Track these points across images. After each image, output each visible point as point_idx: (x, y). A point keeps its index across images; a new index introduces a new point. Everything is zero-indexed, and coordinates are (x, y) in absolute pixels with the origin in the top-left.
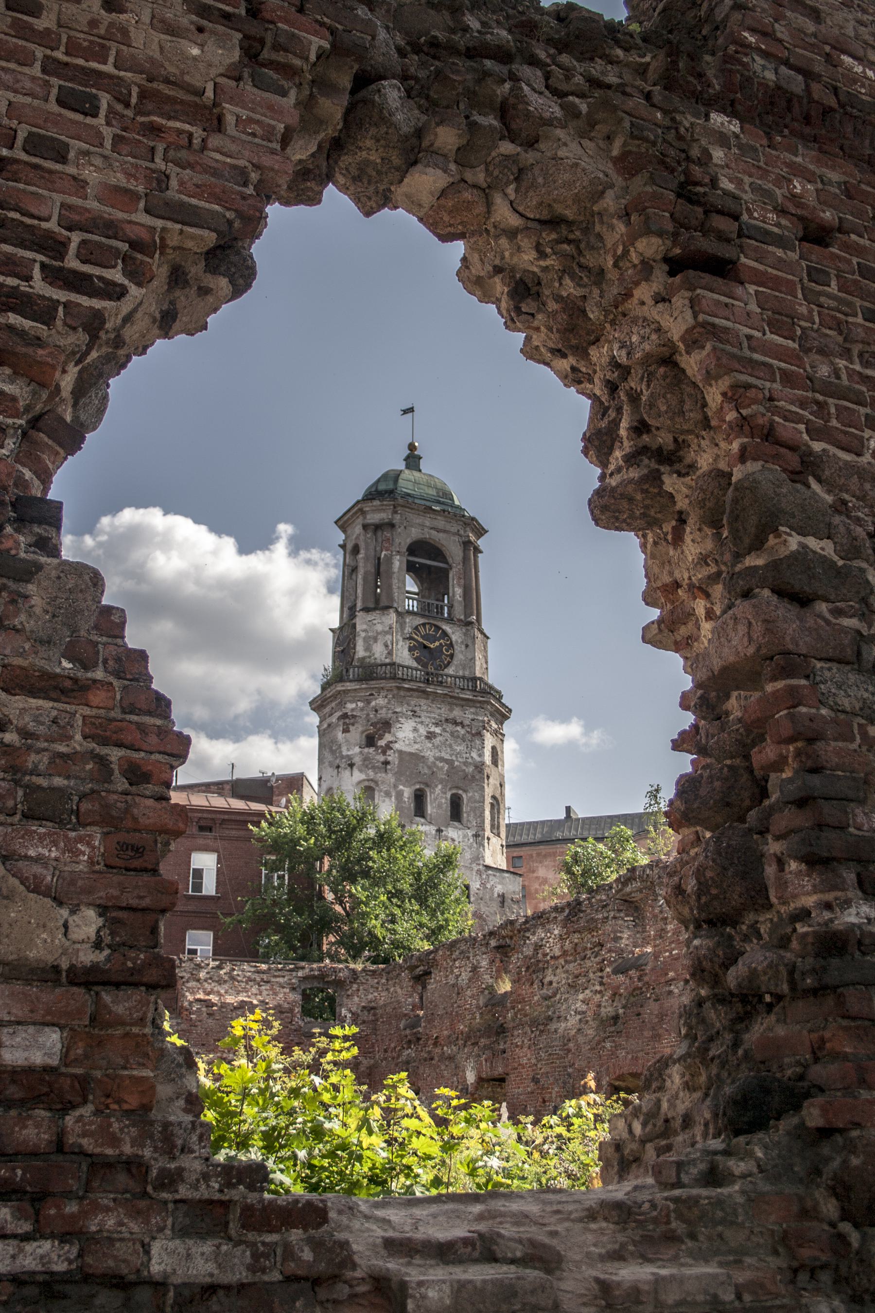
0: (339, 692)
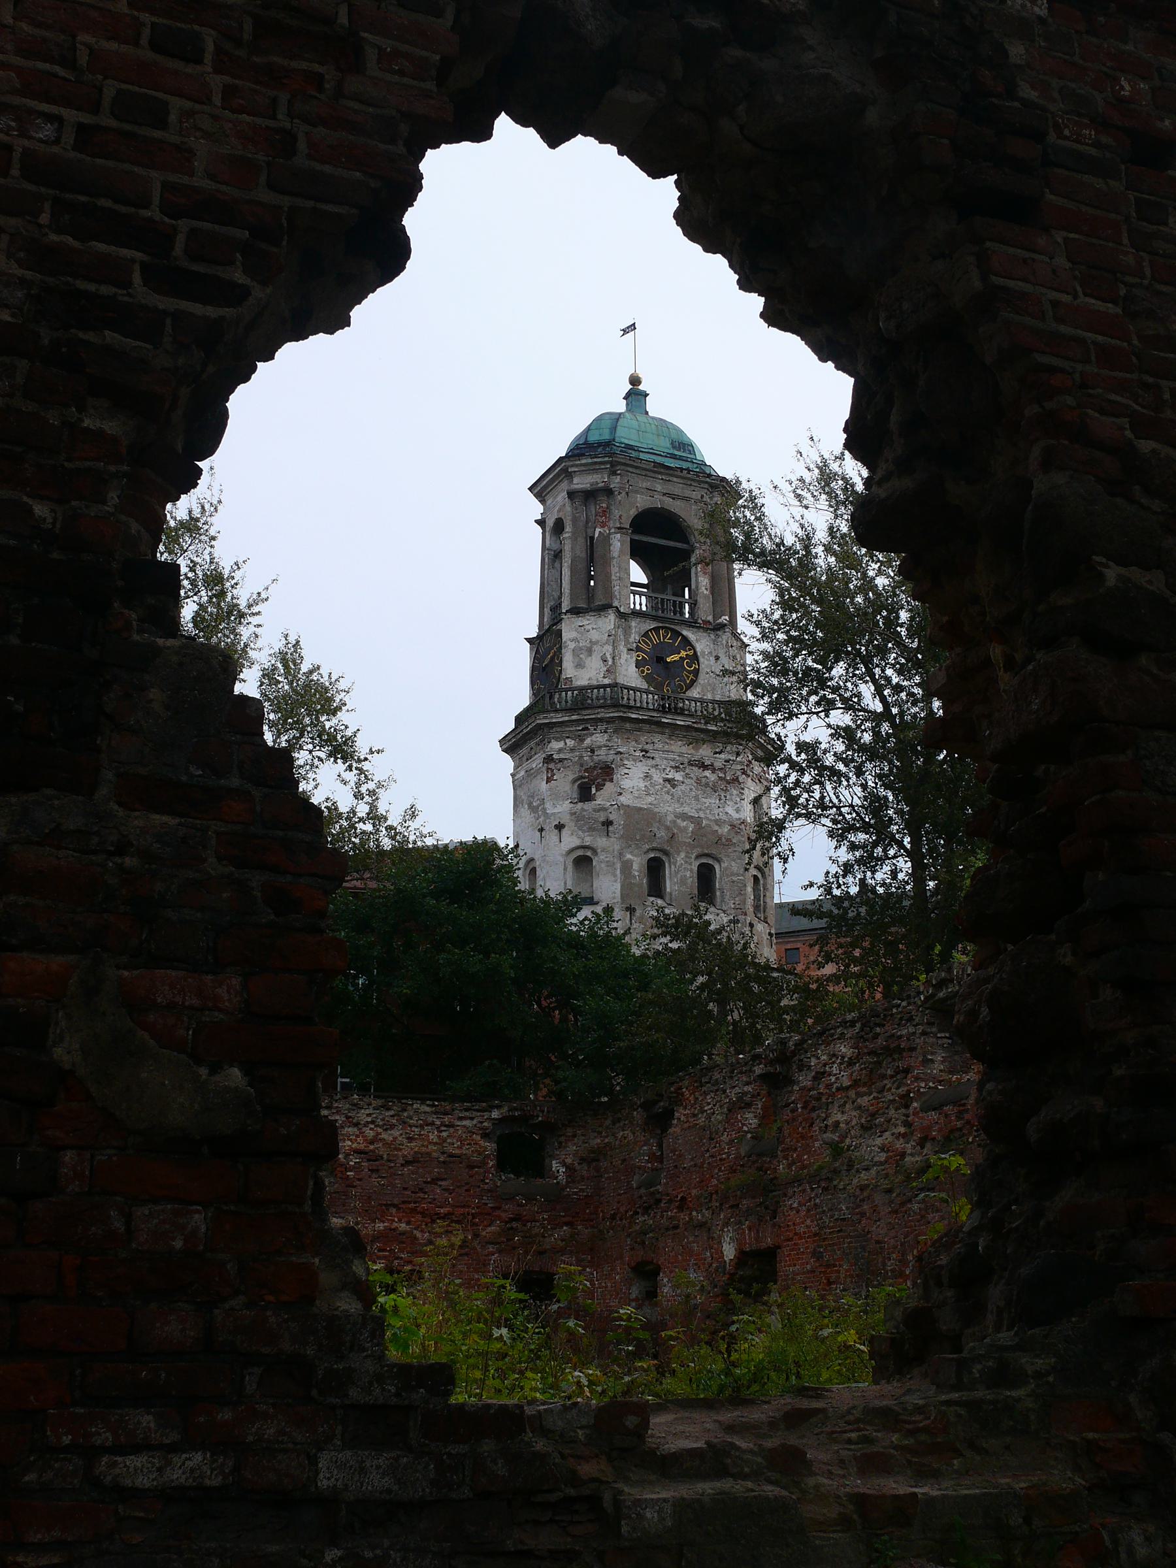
0: (540, 727)
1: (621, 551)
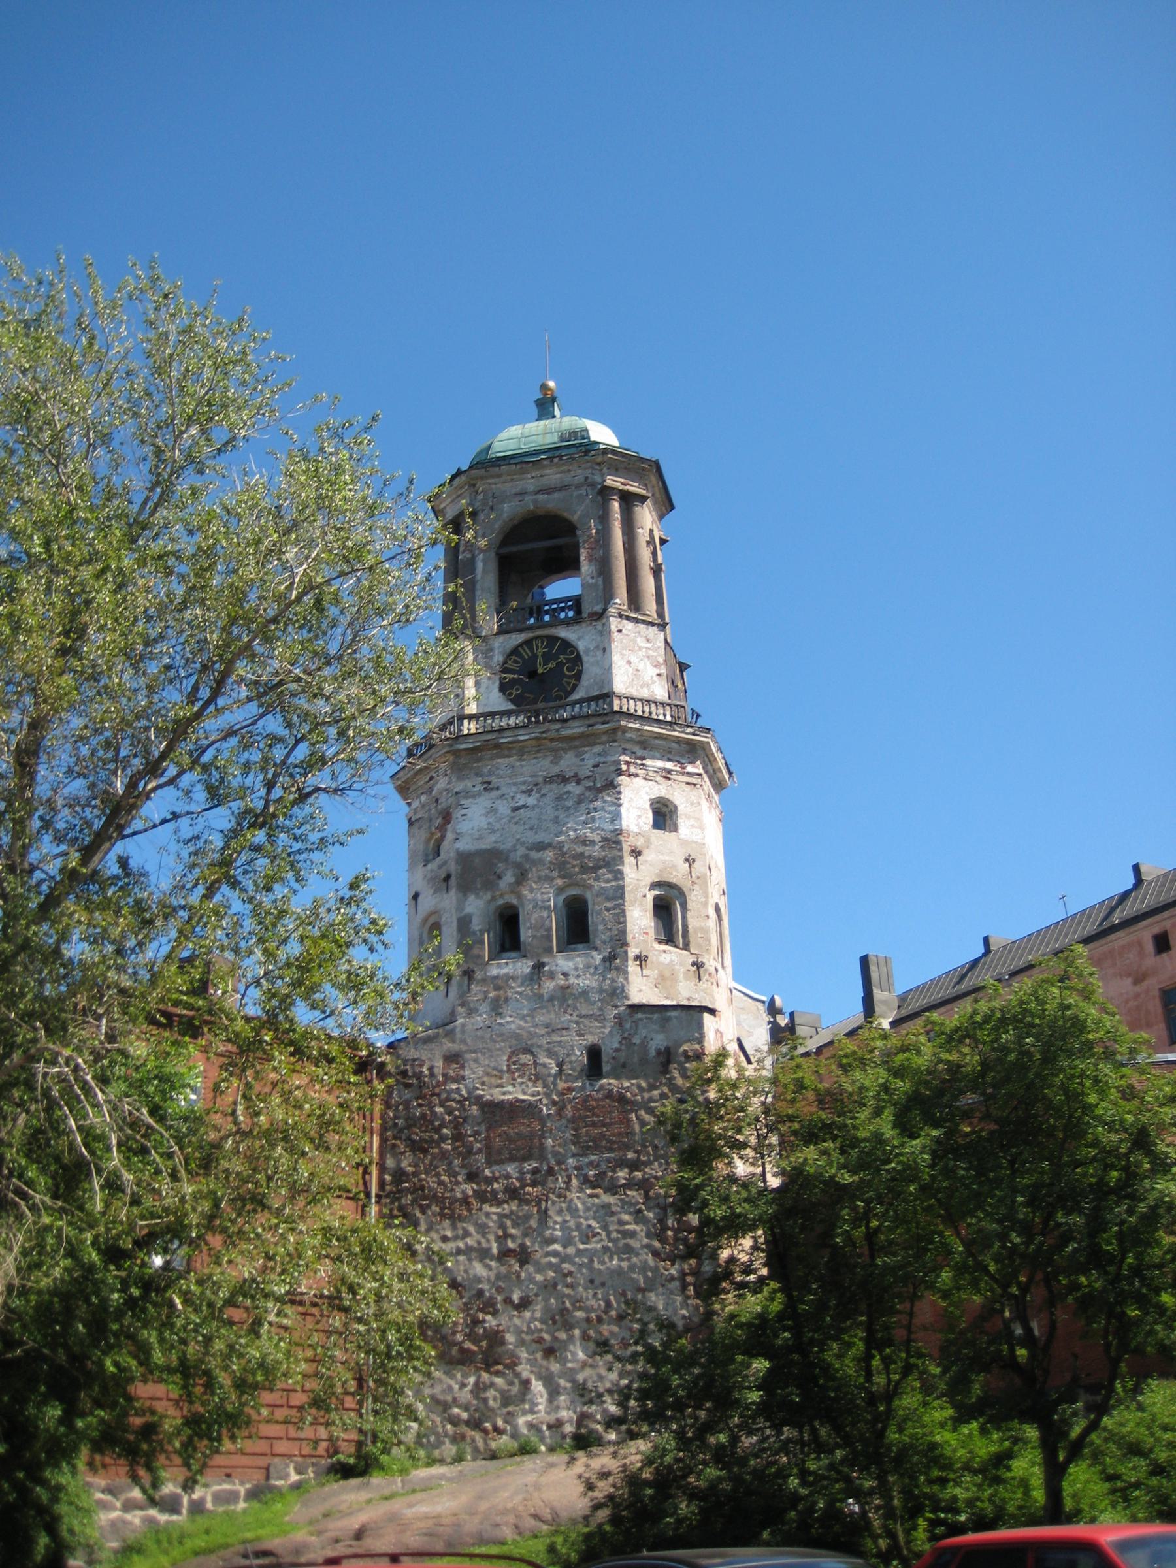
1: (484, 571)
